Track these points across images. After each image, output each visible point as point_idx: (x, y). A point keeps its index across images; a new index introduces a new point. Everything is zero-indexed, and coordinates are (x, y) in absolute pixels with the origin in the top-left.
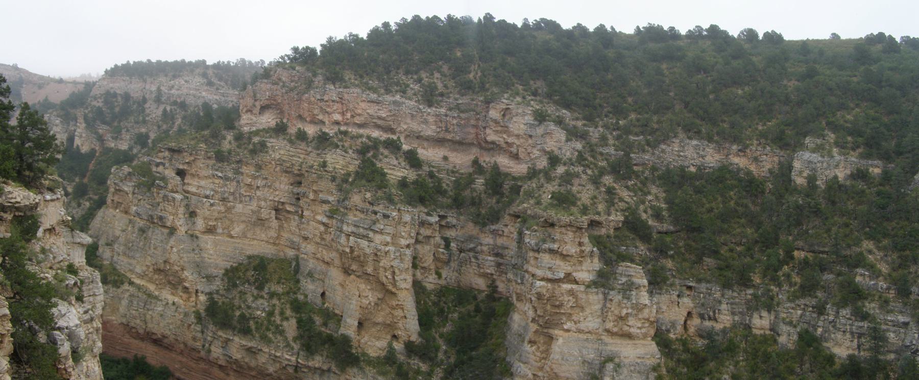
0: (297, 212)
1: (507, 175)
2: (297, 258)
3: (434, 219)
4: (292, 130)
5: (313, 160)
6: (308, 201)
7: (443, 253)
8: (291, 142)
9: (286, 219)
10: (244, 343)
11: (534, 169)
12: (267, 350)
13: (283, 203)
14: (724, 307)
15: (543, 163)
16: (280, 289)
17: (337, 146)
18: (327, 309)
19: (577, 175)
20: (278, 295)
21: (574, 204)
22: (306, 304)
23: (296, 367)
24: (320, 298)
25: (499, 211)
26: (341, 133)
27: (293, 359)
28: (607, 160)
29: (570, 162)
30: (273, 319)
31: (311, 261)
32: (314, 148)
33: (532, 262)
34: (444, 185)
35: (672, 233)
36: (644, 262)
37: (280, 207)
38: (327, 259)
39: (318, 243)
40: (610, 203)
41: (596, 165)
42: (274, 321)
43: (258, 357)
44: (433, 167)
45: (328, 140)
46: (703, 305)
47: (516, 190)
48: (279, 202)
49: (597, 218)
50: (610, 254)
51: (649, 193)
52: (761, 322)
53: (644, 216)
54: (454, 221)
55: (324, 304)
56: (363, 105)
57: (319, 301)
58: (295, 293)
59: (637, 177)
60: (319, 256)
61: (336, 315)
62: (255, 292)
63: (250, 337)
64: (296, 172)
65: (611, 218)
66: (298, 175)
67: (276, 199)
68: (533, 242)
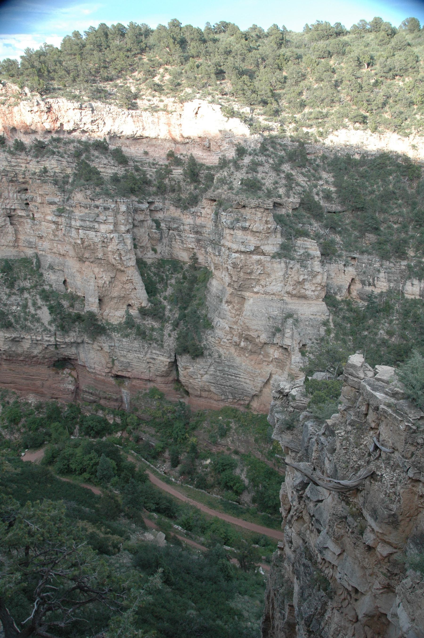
0: (28, 216)
1: (202, 165)
2: (37, 256)
3: (145, 206)
4: (11, 142)
5: (34, 167)
6: (37, 204)
7: (156, 233)
8: (10, 152)
9: (20, 223)
10: (8, 335)
11: (224, 160)
12: (29, 337)
13: (15, 210)
14: (382, 275)
15: (231, 154)
16: (27, 284)
17: (54, 153)
18: (71, 293)
19: (261, 164)
20: (27, 289)
21: (260, 189)
22: (53, 292)
23: (56, 345)
24: (63, 286)
25: (197, 196)
26: (54, 140)
27: (52, 339)
28: (284, 150)
29: (255, 153)
30: (27, 310)
31: (49, 256)
32: (33, 157)
33: (228, 237)
34: (148, 176)
35: (340, 212)
36: (317, 237)
37: (13, 213)
38: (62, 252)
39: (52, 240)
40: (289, 188)
41: (276, 156)
42: (29, 312)
43: (22, 344)
44: (137, 162)
45: (43, 148)
46: (364, 273)
47: (211, 178)
48: (10, 209)
49: (278, 200)
50: (289, 228)
51: (320, 178)
53: (316, 198)
54: (161, 205)
55: (67, 289)
56: (71, 112)
57: (62, 288)
58: (41, 285)
60: (55, 250)
61: (79, 297)
62: (8, 291)
63: (11, 329)
64: (21, 180)
65: (291, 200)
66: (24, 183)
67: (8, 207)
68: (228, 222)
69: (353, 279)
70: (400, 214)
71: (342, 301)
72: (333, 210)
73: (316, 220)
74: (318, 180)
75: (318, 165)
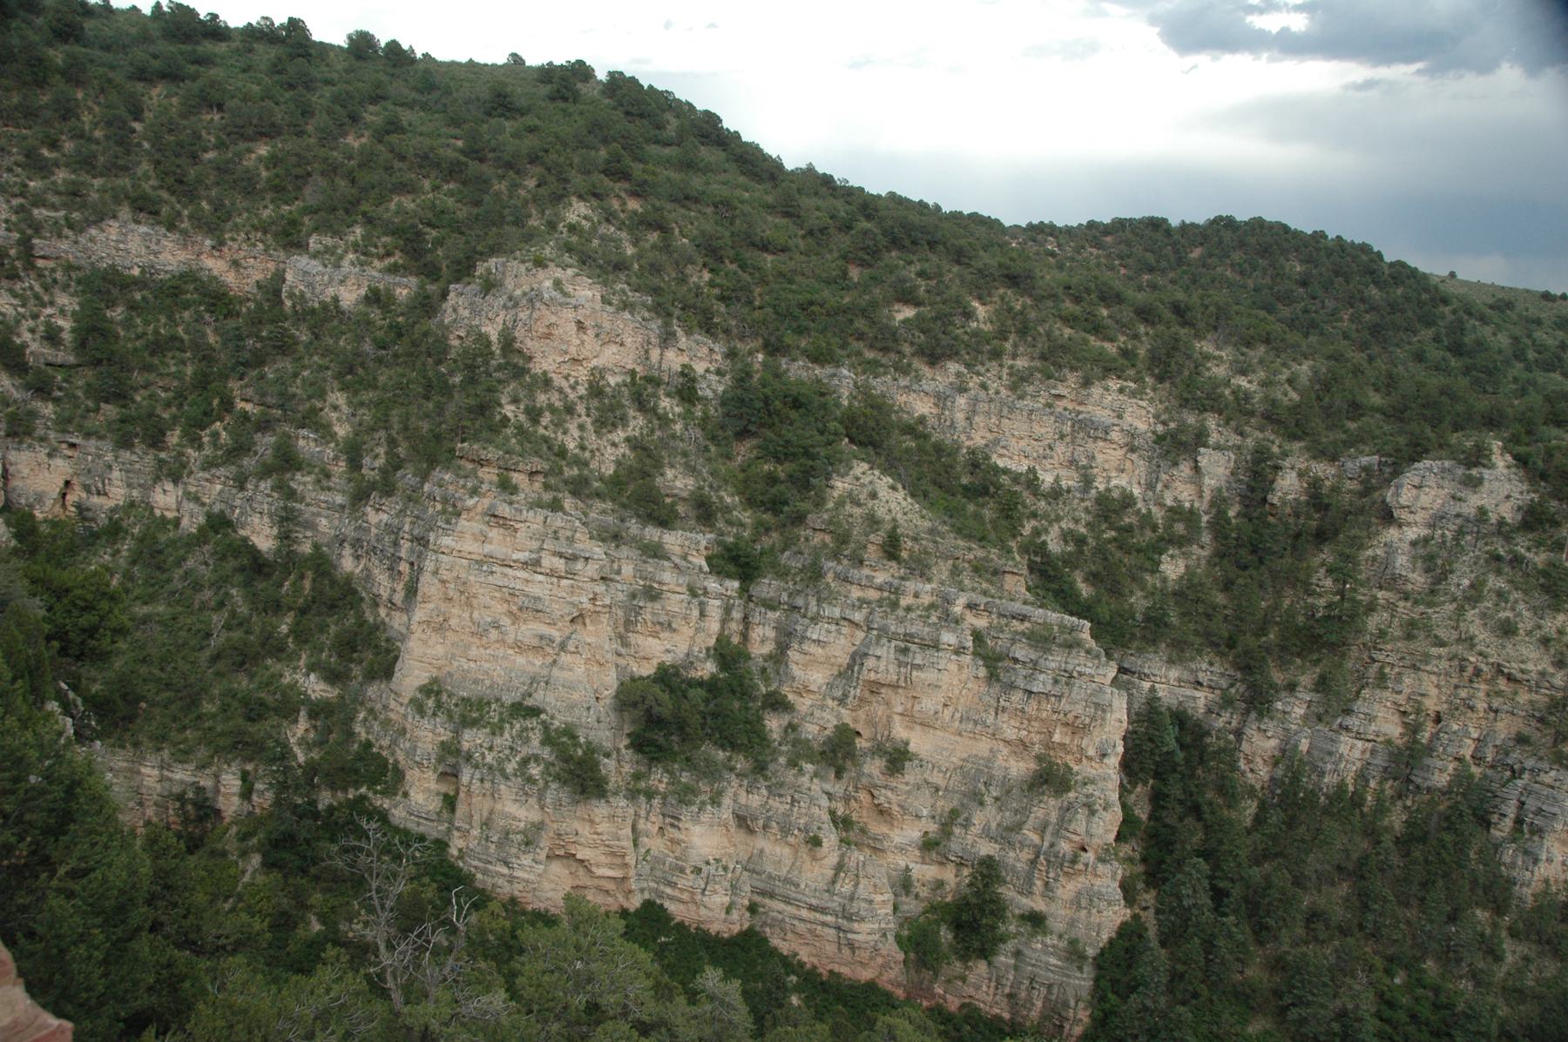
14: (116, 474)
35: (71, 367)
51: (52, 303)
52: (166, 498)
59: (40, 276)
69: (67, 483)
70: (179, 376)
71: (45, 521)
72: (59, 361)
73: (11, 375)
74: (44, 305)
75: (55, 281)
